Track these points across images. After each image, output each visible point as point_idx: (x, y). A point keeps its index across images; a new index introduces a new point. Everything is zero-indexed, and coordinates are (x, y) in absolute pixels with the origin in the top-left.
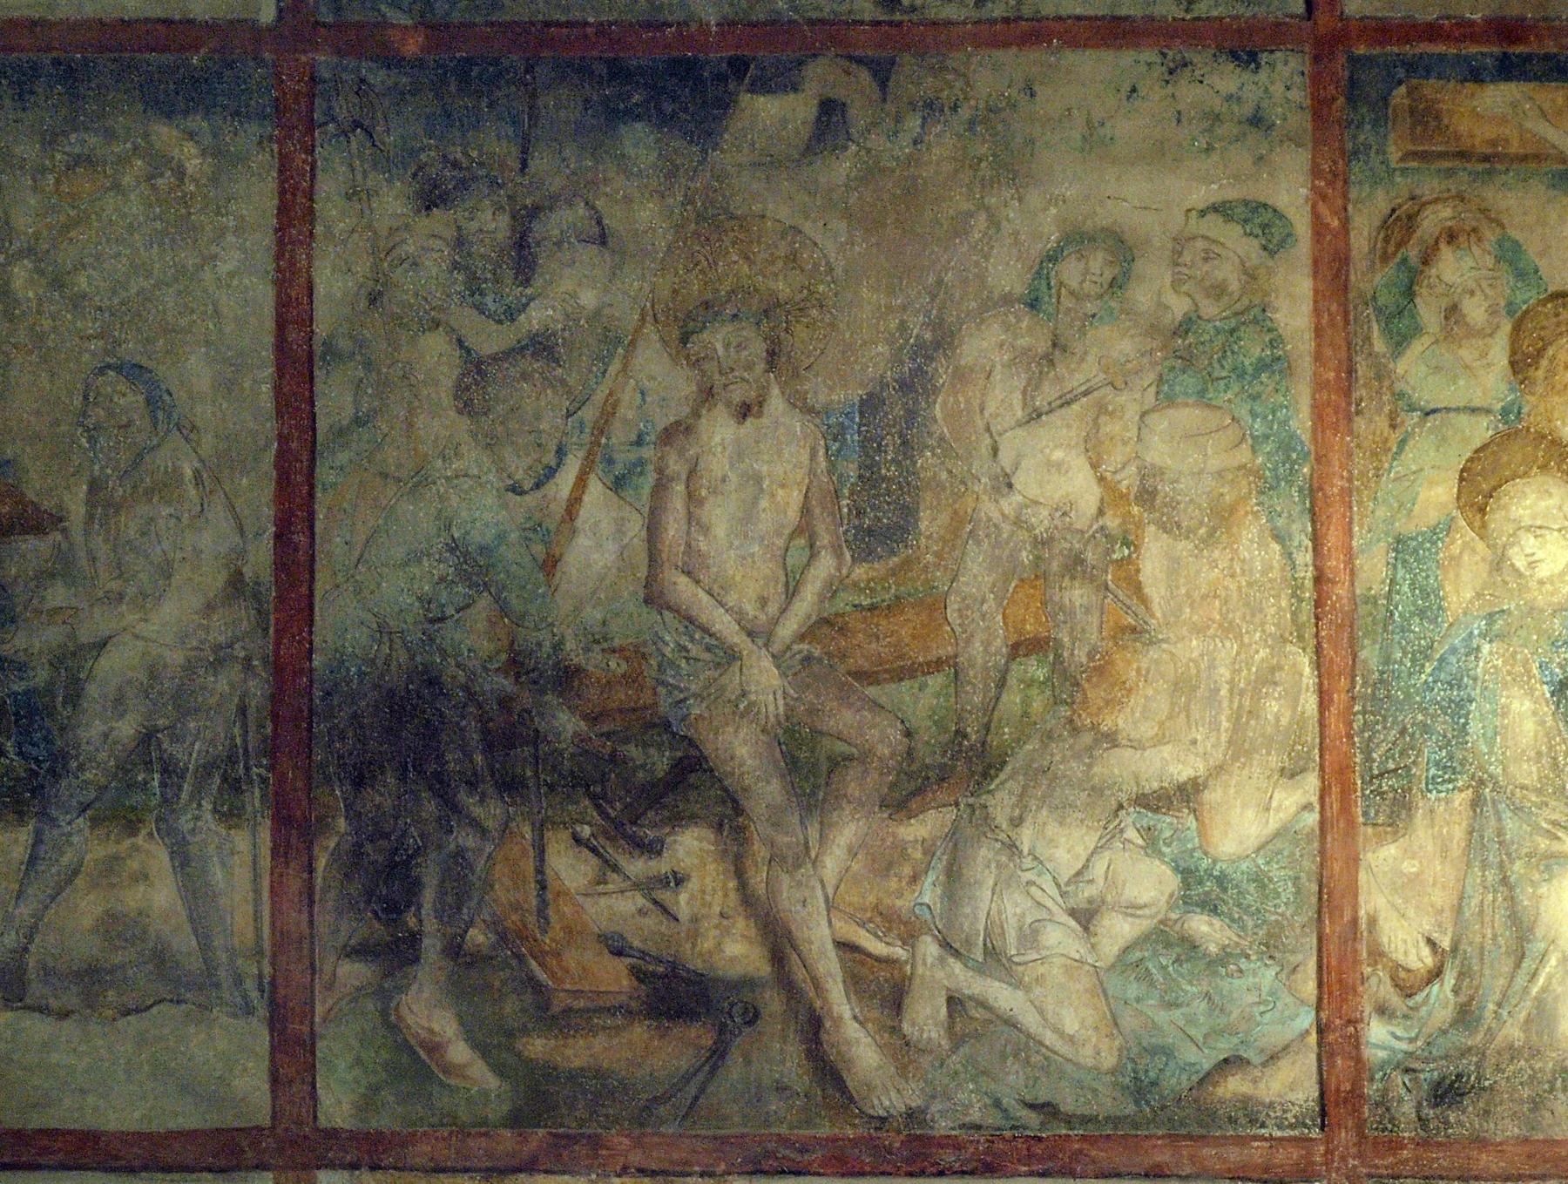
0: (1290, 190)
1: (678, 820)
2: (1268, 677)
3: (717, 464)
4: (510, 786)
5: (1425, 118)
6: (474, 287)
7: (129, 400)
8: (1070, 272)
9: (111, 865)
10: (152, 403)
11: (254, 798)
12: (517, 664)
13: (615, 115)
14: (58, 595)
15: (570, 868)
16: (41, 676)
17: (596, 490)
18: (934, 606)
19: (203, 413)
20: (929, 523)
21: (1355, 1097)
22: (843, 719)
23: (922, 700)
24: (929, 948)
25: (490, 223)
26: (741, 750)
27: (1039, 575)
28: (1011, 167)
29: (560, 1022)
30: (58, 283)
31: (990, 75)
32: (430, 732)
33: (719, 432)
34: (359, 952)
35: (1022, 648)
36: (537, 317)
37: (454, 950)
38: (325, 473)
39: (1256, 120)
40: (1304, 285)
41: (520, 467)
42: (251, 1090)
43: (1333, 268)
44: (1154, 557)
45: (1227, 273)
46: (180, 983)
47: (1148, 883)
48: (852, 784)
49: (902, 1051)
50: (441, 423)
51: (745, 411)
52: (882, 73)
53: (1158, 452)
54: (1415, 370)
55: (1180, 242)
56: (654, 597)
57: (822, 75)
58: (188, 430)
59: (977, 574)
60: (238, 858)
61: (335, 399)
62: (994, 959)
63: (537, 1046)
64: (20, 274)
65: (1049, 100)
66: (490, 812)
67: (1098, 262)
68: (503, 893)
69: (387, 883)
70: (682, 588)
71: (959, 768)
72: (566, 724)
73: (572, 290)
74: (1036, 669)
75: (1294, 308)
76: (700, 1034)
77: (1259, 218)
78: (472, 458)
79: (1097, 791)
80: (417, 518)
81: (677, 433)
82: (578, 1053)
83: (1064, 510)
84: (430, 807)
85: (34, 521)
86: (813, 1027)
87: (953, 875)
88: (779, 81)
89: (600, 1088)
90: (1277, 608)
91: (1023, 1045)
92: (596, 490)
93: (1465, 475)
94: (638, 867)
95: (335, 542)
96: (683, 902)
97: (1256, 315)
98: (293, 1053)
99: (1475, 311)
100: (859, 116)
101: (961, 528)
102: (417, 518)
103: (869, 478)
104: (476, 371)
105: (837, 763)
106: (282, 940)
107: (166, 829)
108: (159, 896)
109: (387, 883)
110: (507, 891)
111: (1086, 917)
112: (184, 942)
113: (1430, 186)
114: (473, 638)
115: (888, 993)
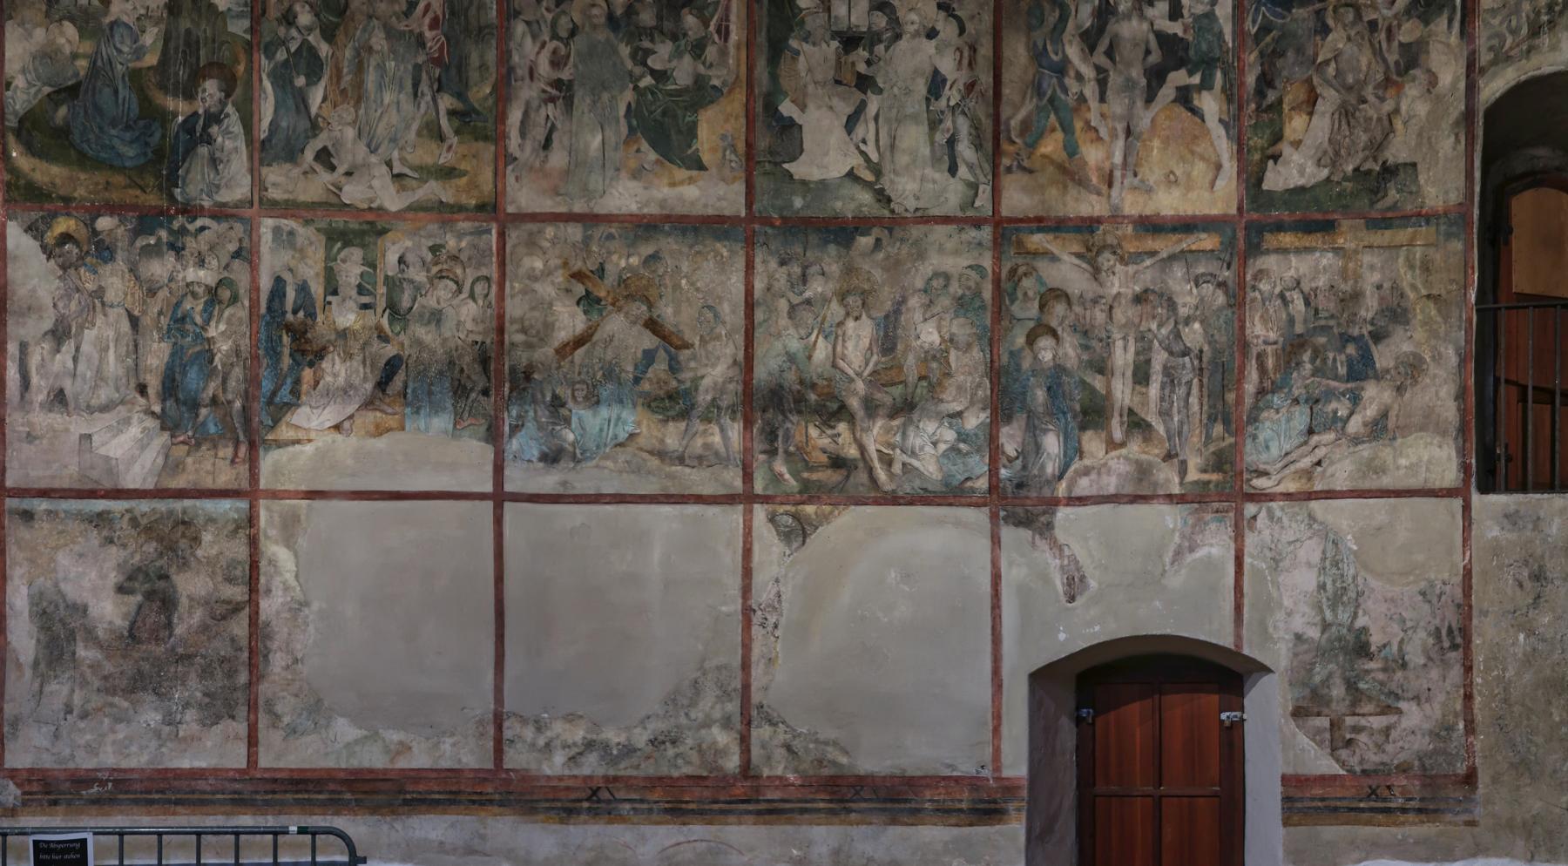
0: (987, 262)
1: (839, 420)
2: (979, 385)
3: (850, 332)
4: (800, 412)
5: (1020, 243)
6: (792, 286)
7: (710, 315)
8: (934, 283)
9: (705, 431)
10: (716, 316)
11: (739, 415)
12: (801, 382)
13: (826, 242)
14: (693, 364)
15: (814, 432)
16: (688, 384)
17: (821, 339)
18: (900, 368)
19: (727, 319)
20: (899, 347)
21: (997, 487)
22: (878, 396)
23: (897, 391)
24: (898, 451)
25: (797, 270)
26: (854, 403)
27: (925, 360)
28: (921, 256)
29: (810, 469)
30: (692, 284)
31: (916, 231)
32: (781, 399)
33: (850, 324)
34: (764, 452)
35: (921, 378)
36: (808, 294)
37: (786, 452)
38: (756, 335)
39: (980, 244)
40: (990, 287)
41: (803, 332)
42: (738, 484)
43: (997, 282)
44: (953, 355)
45: (972, 284)
46: (722, 460)
47: (950, 435)
48: (881, 412)
49: (891, 476)
50: (784, 321)
51: (857, 319)
52: (891, 231)
53: (954, 330)
54: (1016, 309)
55: (961, 275)
56: (834, 365)
57: (876, 232)
58: (724, 323)
59: (911, 361)
60: (735, 431)
61: (759, 315)
62: (913, 454)
63: (805, 475)
64: (684, 282)
65: (931, 238)
66: (794, 418)
67: (941, 281)
68: (798, 438)
69: (771, 435)
70: (841, 363)
71: (906, 408)
72: (813, 397)
73: (816, 287)
74: (925, 384)
75: (987, 294)
76: (844, 472)
77: (978, 268)
78: (792, 331)
79: (938, 413)
80: (778, 345)
81: (840, 324)
82: (815, 476)
83: (931, 344)
84: (781, 417)
85: (687, 346)
86: (870, 470)
87: (904, 434)
88: (865, 233)
89: (820, 486)
90: (982, 368)
91: (920, 474)
92: (821, 339)
93: (1028, 336)
94: (829, 432)
95: (759, 352)
96: (840, 440)
97: (977, 293)
98: (748, 477)
99: (1031, 293)
100: (884, 242)
101: (908, 348)
102: (778, 345)
103: (886, 335)
104: (793, 309)
105: (877, 407)
106: (745, 449)
107: (718, 423)
108: (717, 439)
109: (771, 435)
110: (799, 437)
111: (935, 444)
112: (722, 450)
113: (1020, 261)
114: (791, 377)
115: (888, 462)
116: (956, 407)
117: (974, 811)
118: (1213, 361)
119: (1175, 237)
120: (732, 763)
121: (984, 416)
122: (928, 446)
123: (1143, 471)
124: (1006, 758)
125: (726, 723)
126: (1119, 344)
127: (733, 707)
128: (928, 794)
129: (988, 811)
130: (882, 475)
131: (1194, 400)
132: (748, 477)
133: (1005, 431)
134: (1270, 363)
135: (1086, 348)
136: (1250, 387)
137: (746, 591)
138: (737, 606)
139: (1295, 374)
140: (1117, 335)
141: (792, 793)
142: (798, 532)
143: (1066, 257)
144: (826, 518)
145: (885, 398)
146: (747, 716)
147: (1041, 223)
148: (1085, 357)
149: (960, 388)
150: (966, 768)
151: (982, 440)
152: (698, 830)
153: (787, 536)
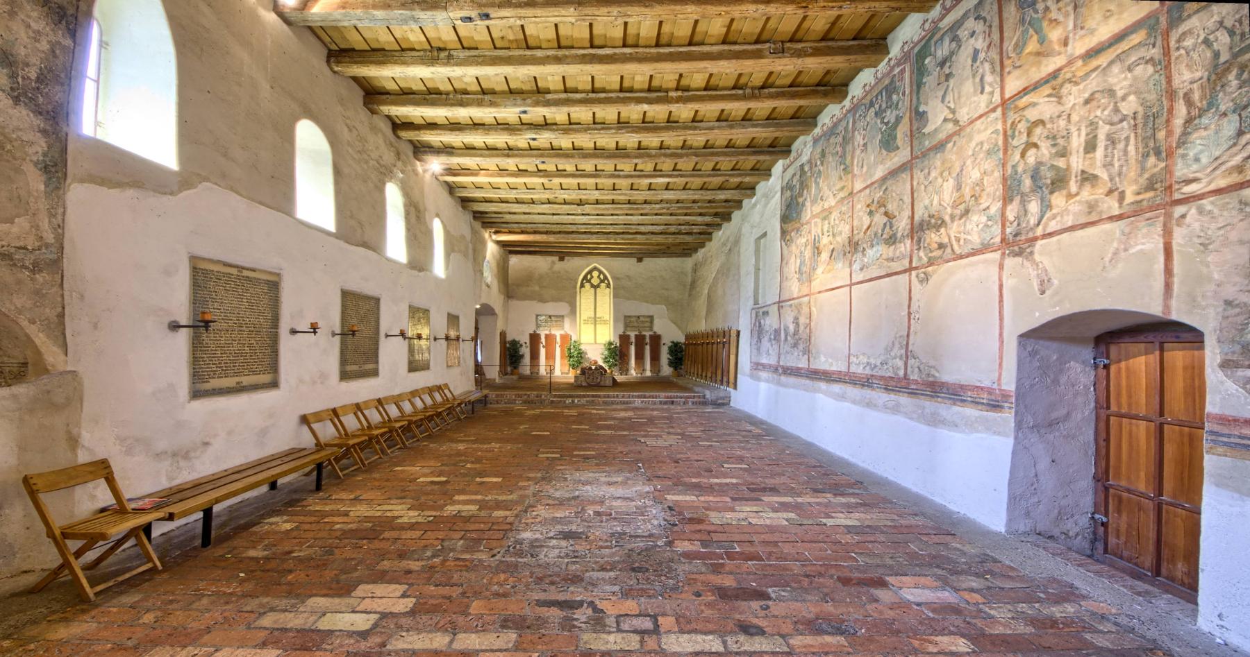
5: (1016, 107)
26: (947, 218)
28: (971, 140)
47: (984, 219)
89: (936, 258)
97: (996, 145)
109: (919, 241)
115: (958, 240)
116: (986, 205)
117: (988, 405)
118: (1146, 117)
119: (1111, 50)
120: (901, 373)
121: (999, 204)
122: (975, 229)
123: (1091, 207)
124: (1004, 380)
125: (901, 358)
126: (1075, 134)
127: (903, 351)
128: (969, 394)
129: (995, 406)
130: (956, 247)
131: (1131, 148)
132: (911, 262)
133: (1009, 208)
134: (1196, 96)
135: (1054, 145)
136: (1178, 122)
137: (909, 306)
138: (906, 313)
139: (1221, 95)
140: (1073, 129)
141: (919, 387)
142: (925, 279)
143: (1041, 101)
144: (934, 272)
145: (958, 212)
146: (908, 355)
147: (1025, 91)
148: (1054, 151)
149: (988, 195)
150: (986, 383)
151: (999, 218)
152: (892, 396)
153: (921, 282)
